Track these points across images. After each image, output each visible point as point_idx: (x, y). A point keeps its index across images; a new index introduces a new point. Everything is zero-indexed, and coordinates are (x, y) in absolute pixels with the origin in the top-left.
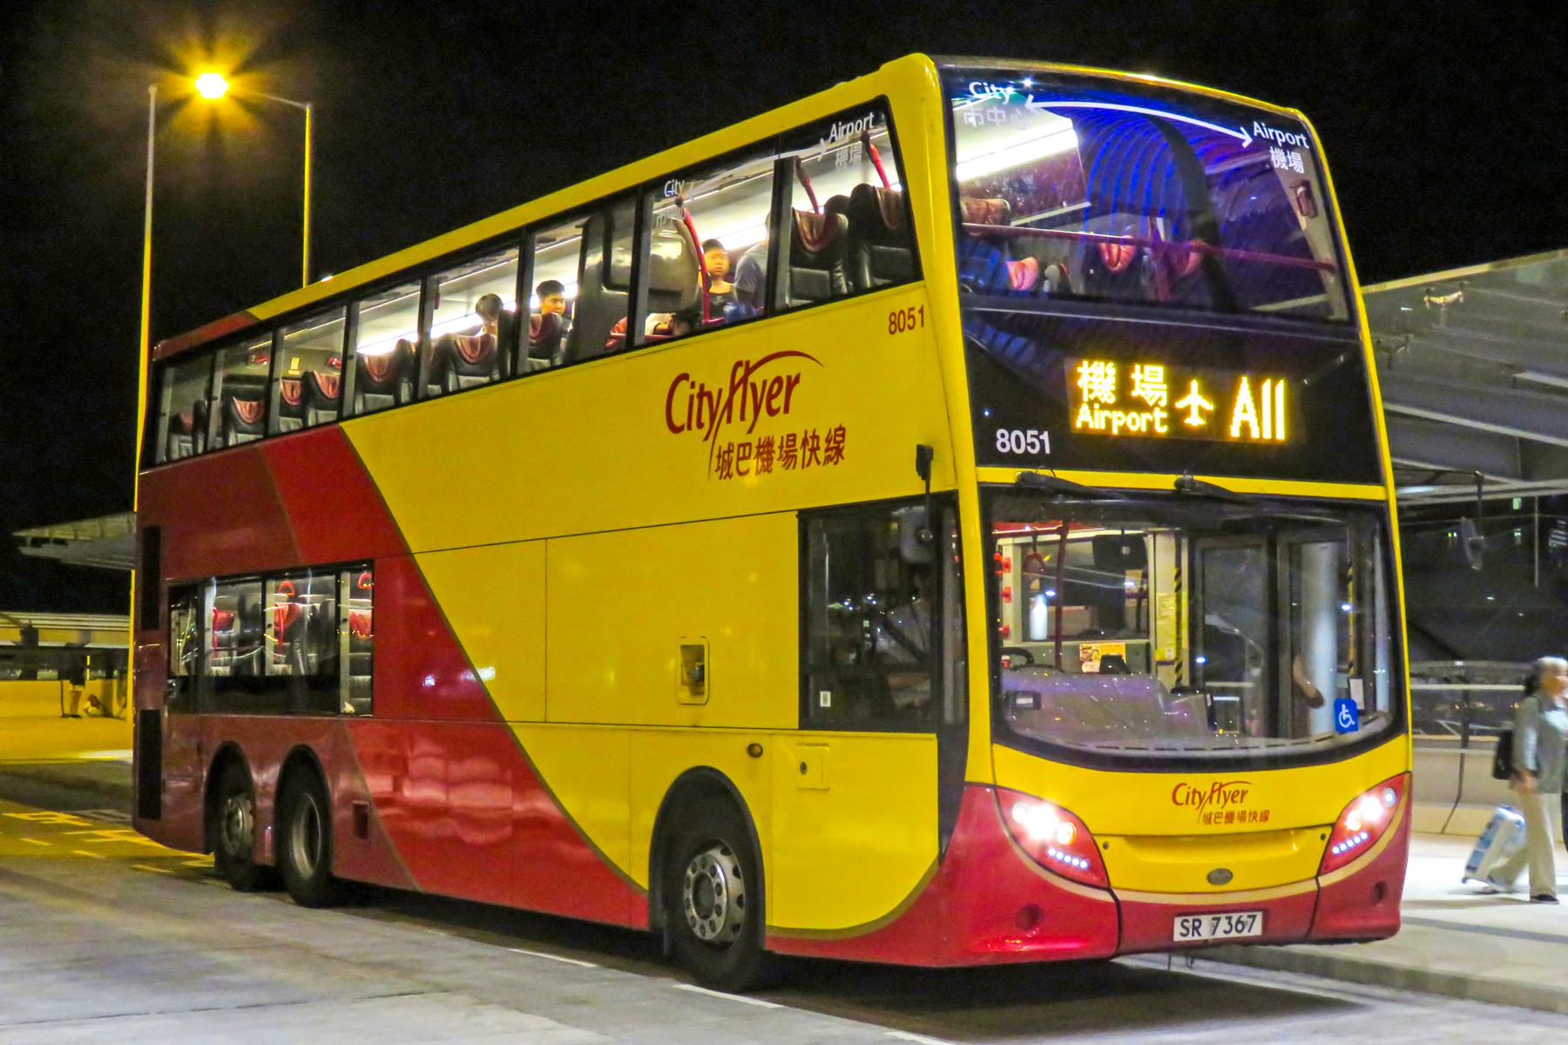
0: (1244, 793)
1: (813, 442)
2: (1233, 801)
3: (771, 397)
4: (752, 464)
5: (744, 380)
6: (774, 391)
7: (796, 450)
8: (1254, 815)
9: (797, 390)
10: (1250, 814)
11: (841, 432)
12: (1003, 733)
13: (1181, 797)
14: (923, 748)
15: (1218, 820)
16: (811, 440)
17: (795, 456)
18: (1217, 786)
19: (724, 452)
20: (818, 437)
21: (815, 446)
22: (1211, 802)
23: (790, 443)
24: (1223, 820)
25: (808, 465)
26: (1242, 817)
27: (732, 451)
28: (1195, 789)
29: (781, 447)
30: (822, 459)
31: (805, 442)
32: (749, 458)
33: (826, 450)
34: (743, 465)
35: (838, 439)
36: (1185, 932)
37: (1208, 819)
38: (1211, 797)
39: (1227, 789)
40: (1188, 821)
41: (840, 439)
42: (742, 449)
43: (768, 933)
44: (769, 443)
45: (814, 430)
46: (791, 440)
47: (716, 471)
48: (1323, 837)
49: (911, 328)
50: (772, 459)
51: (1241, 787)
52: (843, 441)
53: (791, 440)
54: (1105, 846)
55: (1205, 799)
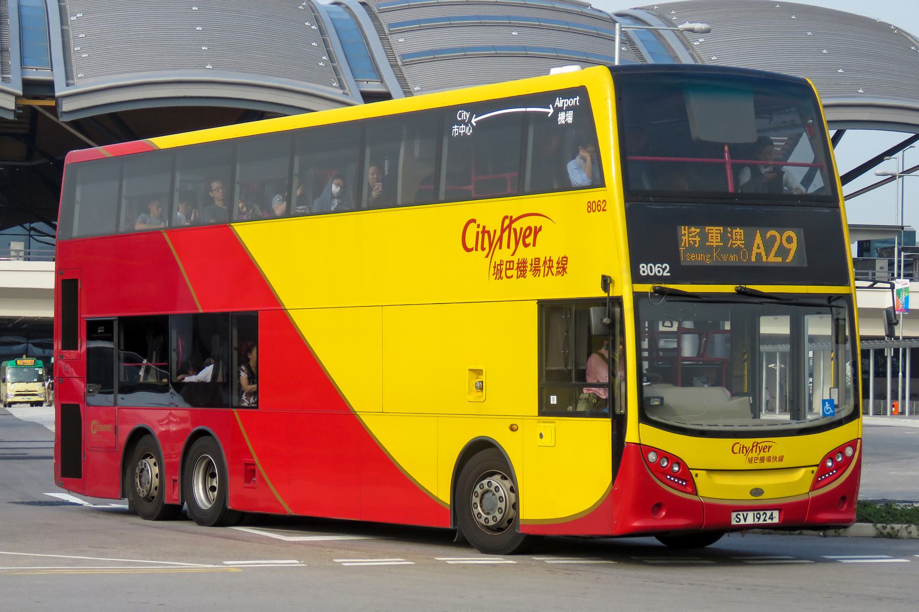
0: (770, 447)
1: (550, 263)
2: (764, 452)
3: (525, 237)
4: (514, 272)
5: (509, 226)
6: (527, 234)
7: (540, 267)
8: (775, 458)
9: (540, 232)
10: (773, 458)
11: (565, 259)
12: (644, 418)
13: (736, 449)
14: (604, 426)
15: (755, 461)
16: (548, 262)
17: (540, 270)
18: (755, 444)
19: (498, 265)
20: (552, 261)
21: (551, 265)
22: (752, 452)
23: (536, 263)
24: (759, 461)
25: (547, 276)
26: (769, 460)
27: (503, 265)
28: (743, 447)
29: (531, 265)
30: (555, 273)
31: (545, 262)
32: (513, 269)
33: (557, 268)
34: (509, 273)
35: (563, 263)
36: (738, 520)
37: (750, 461)
38: (752, 450)
39: (760, 445)
40: (740, 462)
41: (565, 263)
42: (508, 264)
43: (521, 523)
44: (525, 262)
45: (550, 257)
46: (537, 261)
47: (493, 275)
48: (813, 472)
49: (599, 211)
50: (526, 270)
51: (768, 444)
52: (566, 264)
53: (537, 261)
54: (697, 475)
55: (750, 449)
